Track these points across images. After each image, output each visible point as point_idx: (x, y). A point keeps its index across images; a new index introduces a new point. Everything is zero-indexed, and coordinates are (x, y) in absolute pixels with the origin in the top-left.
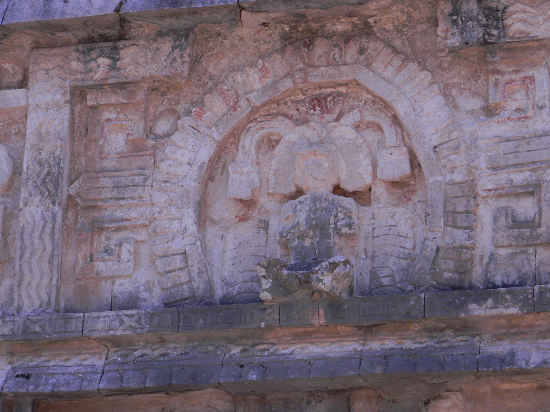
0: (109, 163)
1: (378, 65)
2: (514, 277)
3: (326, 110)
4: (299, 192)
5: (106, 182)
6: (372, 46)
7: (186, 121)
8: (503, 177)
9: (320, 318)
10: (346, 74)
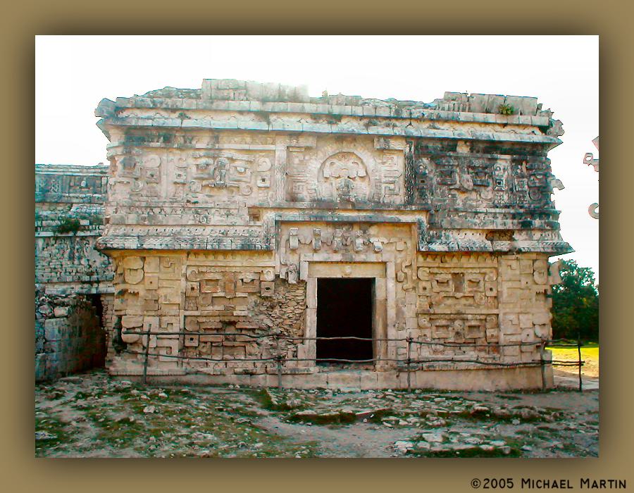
0: (295, 166)
1: (359, 149)
2: (389, 201)
3: (345, 159)
4: (339, 177)
5: (295, 170)
6: (357, 145)
7: (313, 157)
8: (387, 179)
9: (350, 207)
10: (351, 151)
